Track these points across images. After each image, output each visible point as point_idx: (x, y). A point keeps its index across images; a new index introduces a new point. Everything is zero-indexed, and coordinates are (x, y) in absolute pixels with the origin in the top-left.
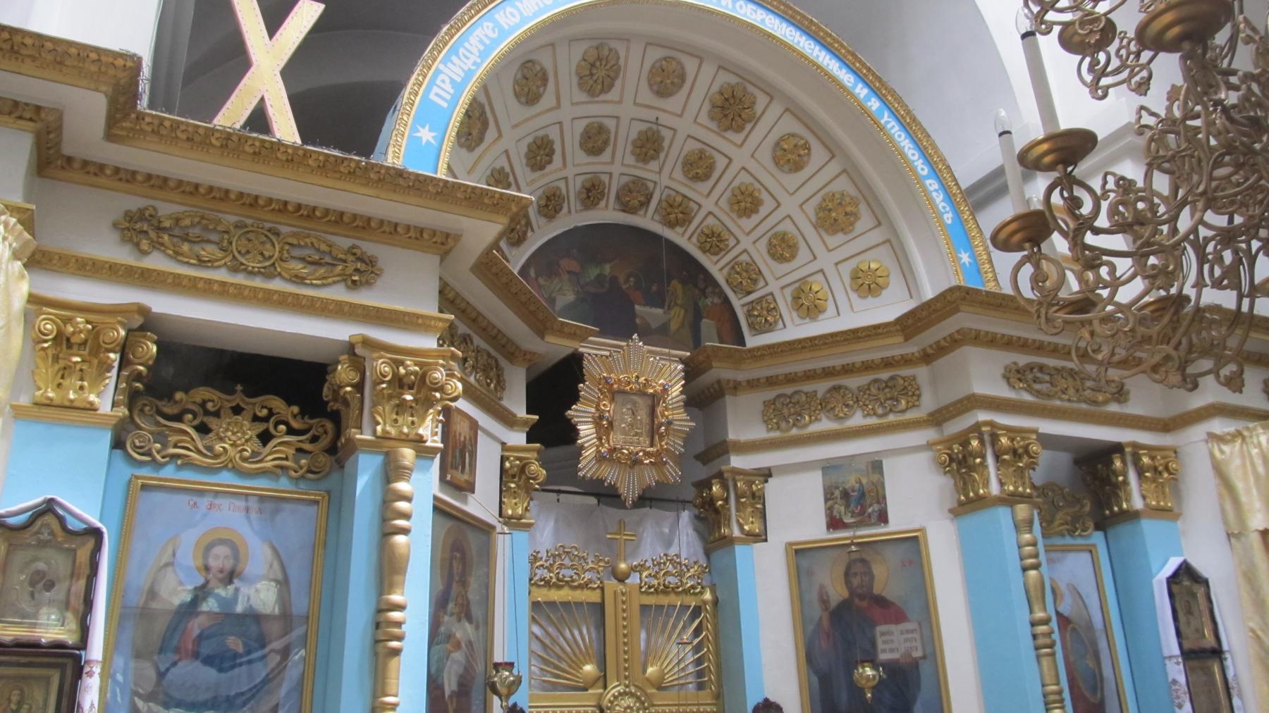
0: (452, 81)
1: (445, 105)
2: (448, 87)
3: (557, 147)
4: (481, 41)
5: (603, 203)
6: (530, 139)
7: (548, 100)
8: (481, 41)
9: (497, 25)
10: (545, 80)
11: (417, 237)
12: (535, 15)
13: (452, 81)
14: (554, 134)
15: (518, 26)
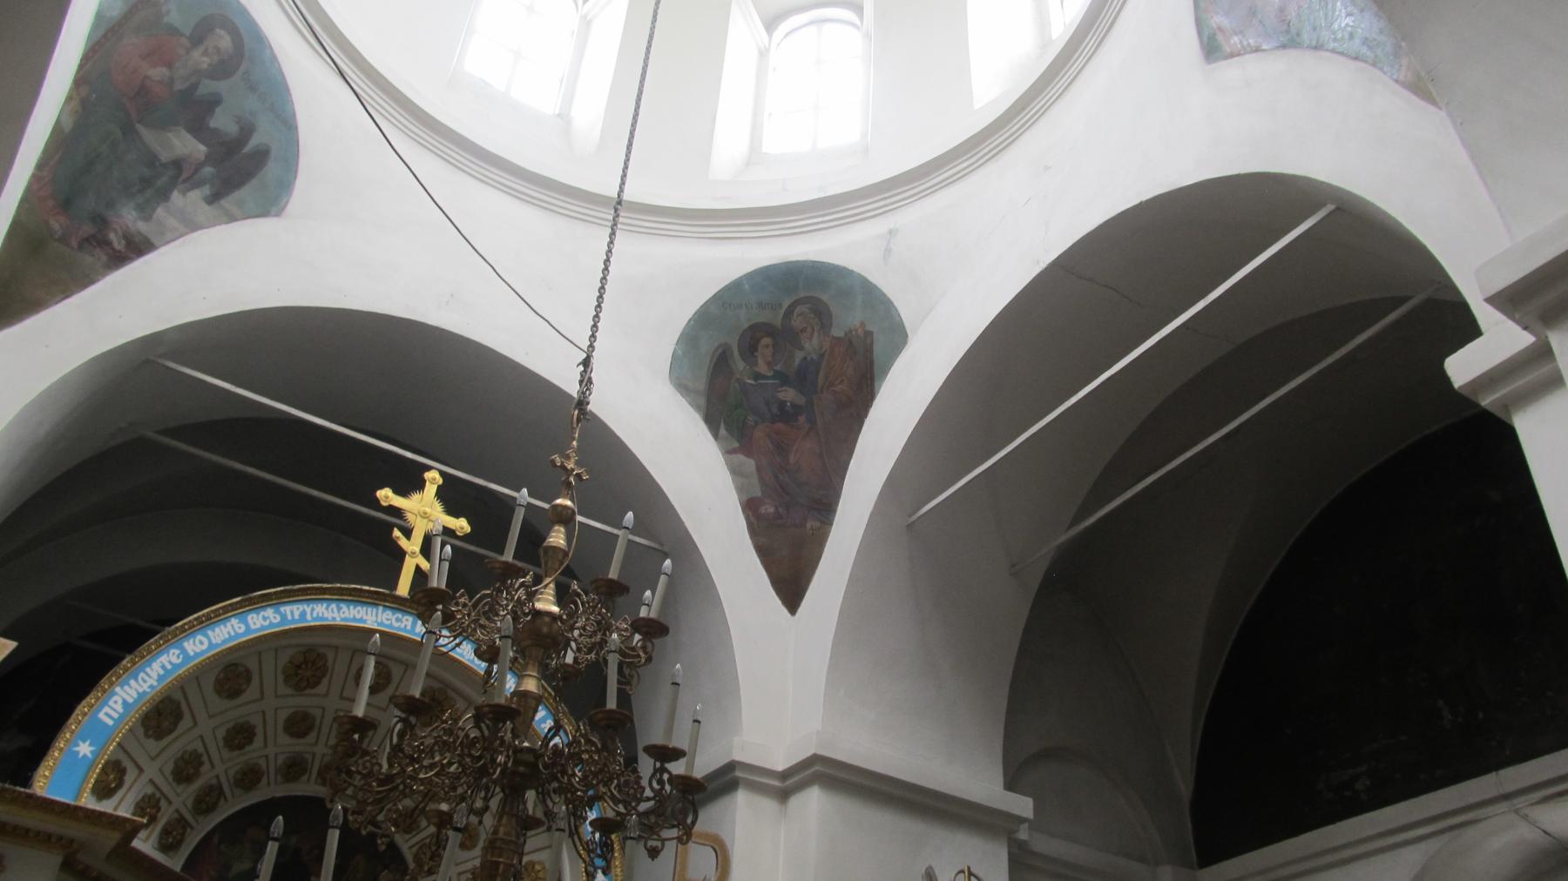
0: (125, 702)
1: (111, 723)
2: (119, 708)
3: (259, 730)
4: (163, 667)
5: (305, 778)
6: (231, 725)
7: (251, 692)
8: (163, 667)
9: (184, 651)
10: (249, 680)
11: (44, 840)
12: (224, 642)
13: (125, 702)
14: (256, 720)
15: (203, 652)
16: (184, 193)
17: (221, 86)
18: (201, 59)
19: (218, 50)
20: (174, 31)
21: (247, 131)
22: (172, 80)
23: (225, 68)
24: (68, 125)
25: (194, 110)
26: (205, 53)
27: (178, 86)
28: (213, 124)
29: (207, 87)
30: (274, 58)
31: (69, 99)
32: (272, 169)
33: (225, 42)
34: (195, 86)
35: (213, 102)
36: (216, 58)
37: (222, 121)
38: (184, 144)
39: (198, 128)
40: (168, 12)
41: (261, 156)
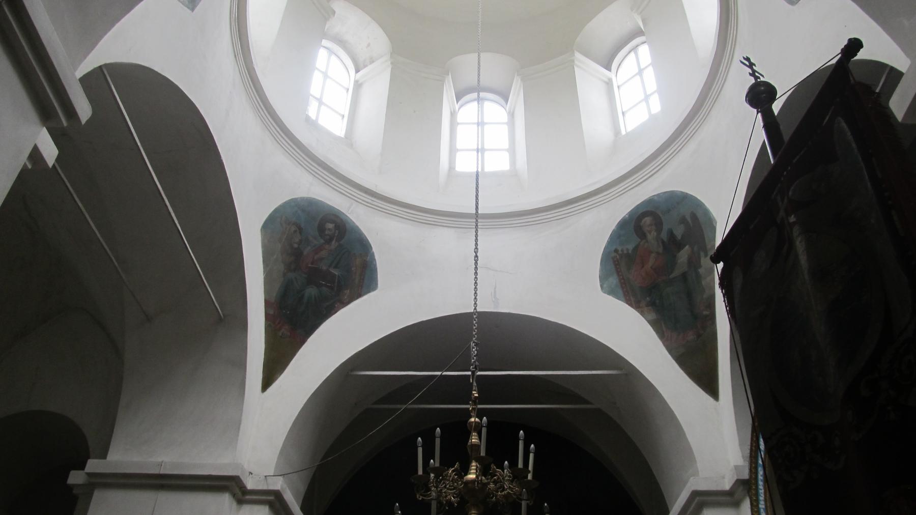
16: (700, 266)
17: (666, 227)
18: (652, 236)
19: (651, 225)
20: (636, 249)
21: (683, 220)
22: (658, 253)
23: (658, 224)
24: (653, 316)
25: (672, 245)
26: (650, 232)
27: (661, 250)
28: (679, 237)
29: (664, 235)
30: (658, 195)
31: (642, 313)
32: (699, 214)
33: (648, 220)
34: (663, 242)
35: (671, 234)
36: (654, 227)
37: (679, 232)
38: (683, 255)
39: (680, 246)
40: (628, 250)
41: (694, 217)
